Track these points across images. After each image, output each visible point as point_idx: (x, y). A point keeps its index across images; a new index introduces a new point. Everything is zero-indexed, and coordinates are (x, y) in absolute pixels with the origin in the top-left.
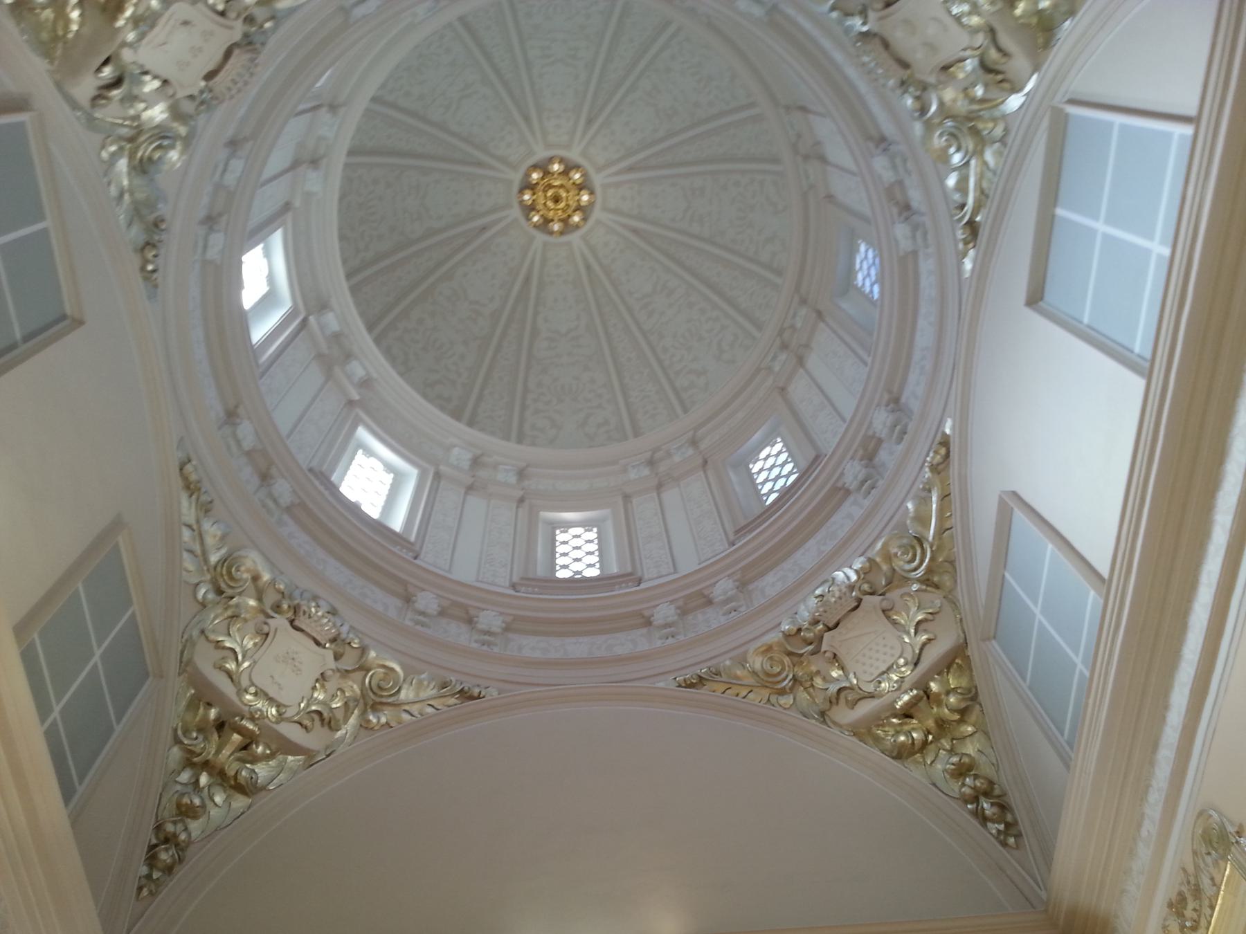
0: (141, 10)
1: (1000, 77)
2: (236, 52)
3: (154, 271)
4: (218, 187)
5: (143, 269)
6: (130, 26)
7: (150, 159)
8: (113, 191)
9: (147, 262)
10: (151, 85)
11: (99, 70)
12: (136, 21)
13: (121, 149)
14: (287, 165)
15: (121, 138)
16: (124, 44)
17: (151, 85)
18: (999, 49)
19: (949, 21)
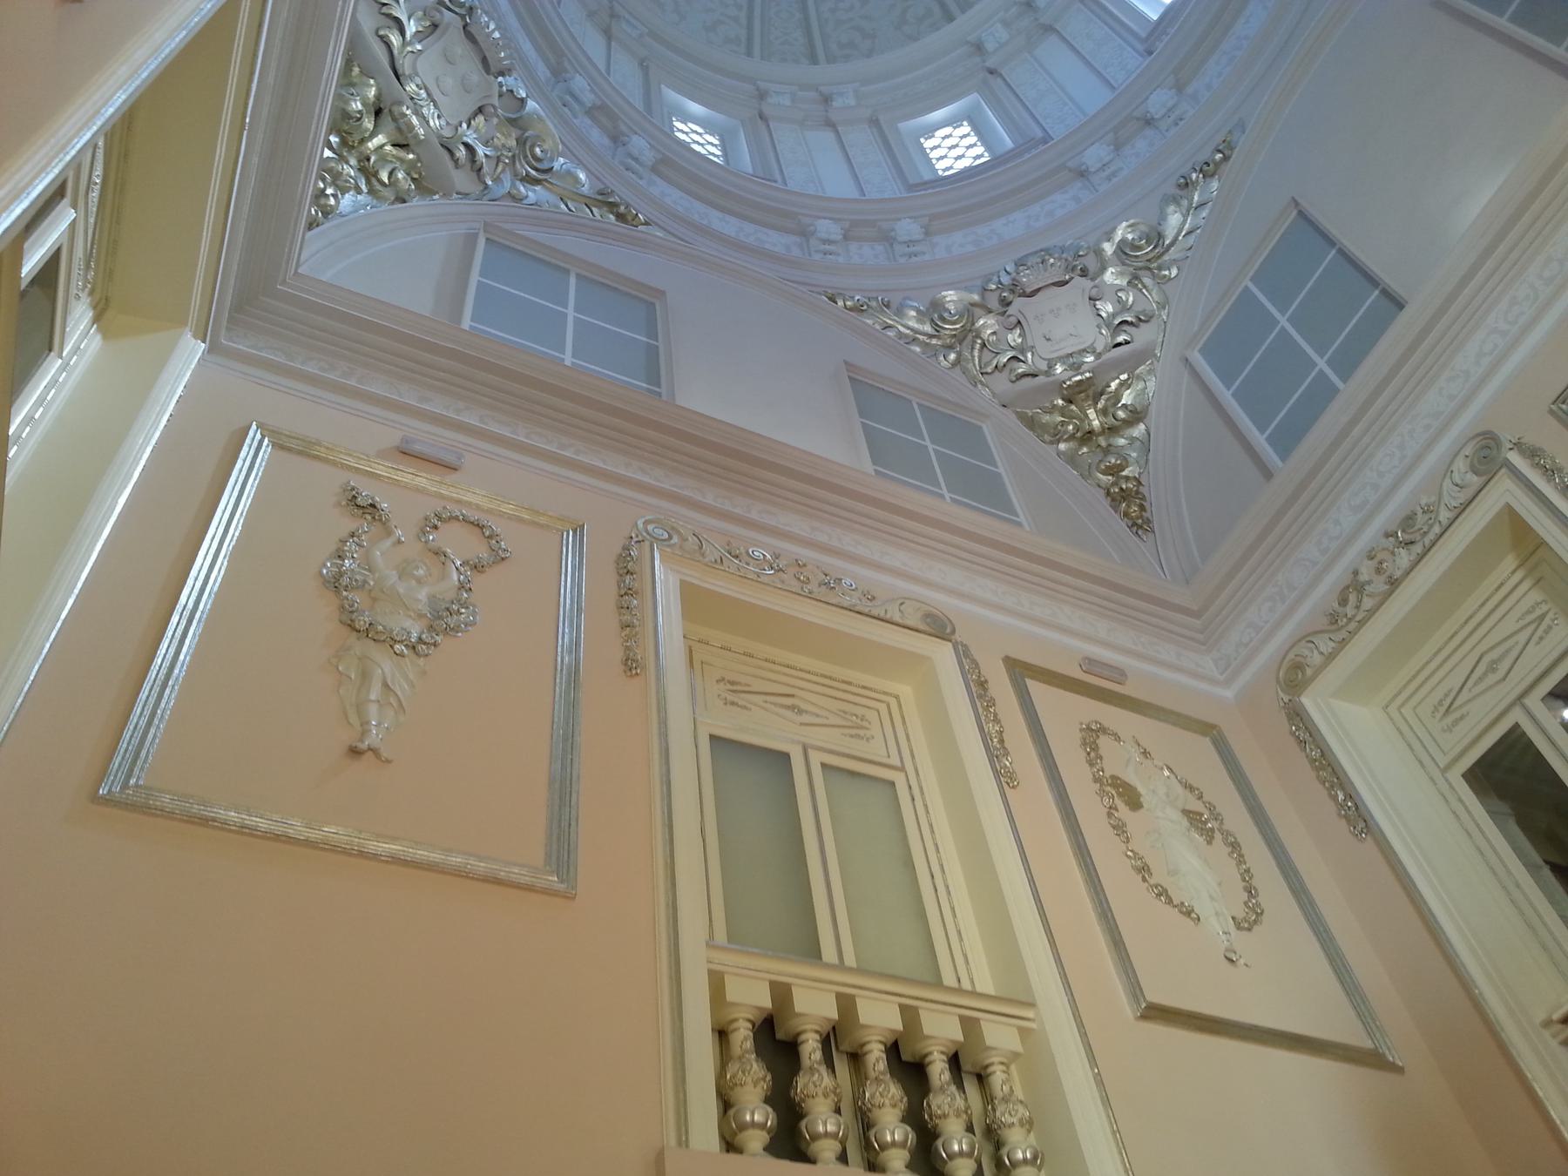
0: (1071, 373)
1: (385, 10)
2: (1028, 290)
3: (1220, 151)
4: (1118, 147)
5: (1226, 159)
6: (1084, 367)
7: (1148, 243)
8: (1191, 240)
9: (1218, 164)
10: (1107, 308)
11: (1127, 342)
12: (1077, 368)
13: (1160, 268)
14: (1053, 38)
15: (1154, 276)
16: (1098, 356)
17: (1107, 308)
18: (388, 45)
19: (436, 95)
